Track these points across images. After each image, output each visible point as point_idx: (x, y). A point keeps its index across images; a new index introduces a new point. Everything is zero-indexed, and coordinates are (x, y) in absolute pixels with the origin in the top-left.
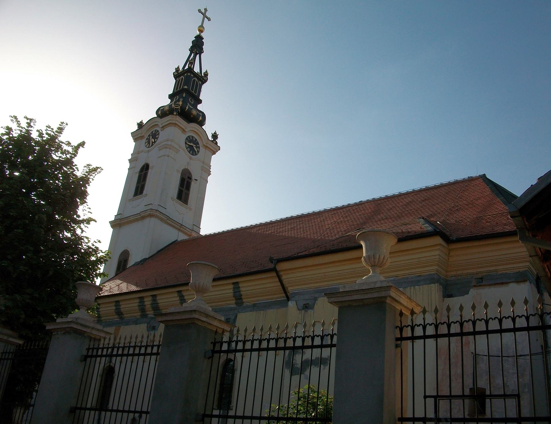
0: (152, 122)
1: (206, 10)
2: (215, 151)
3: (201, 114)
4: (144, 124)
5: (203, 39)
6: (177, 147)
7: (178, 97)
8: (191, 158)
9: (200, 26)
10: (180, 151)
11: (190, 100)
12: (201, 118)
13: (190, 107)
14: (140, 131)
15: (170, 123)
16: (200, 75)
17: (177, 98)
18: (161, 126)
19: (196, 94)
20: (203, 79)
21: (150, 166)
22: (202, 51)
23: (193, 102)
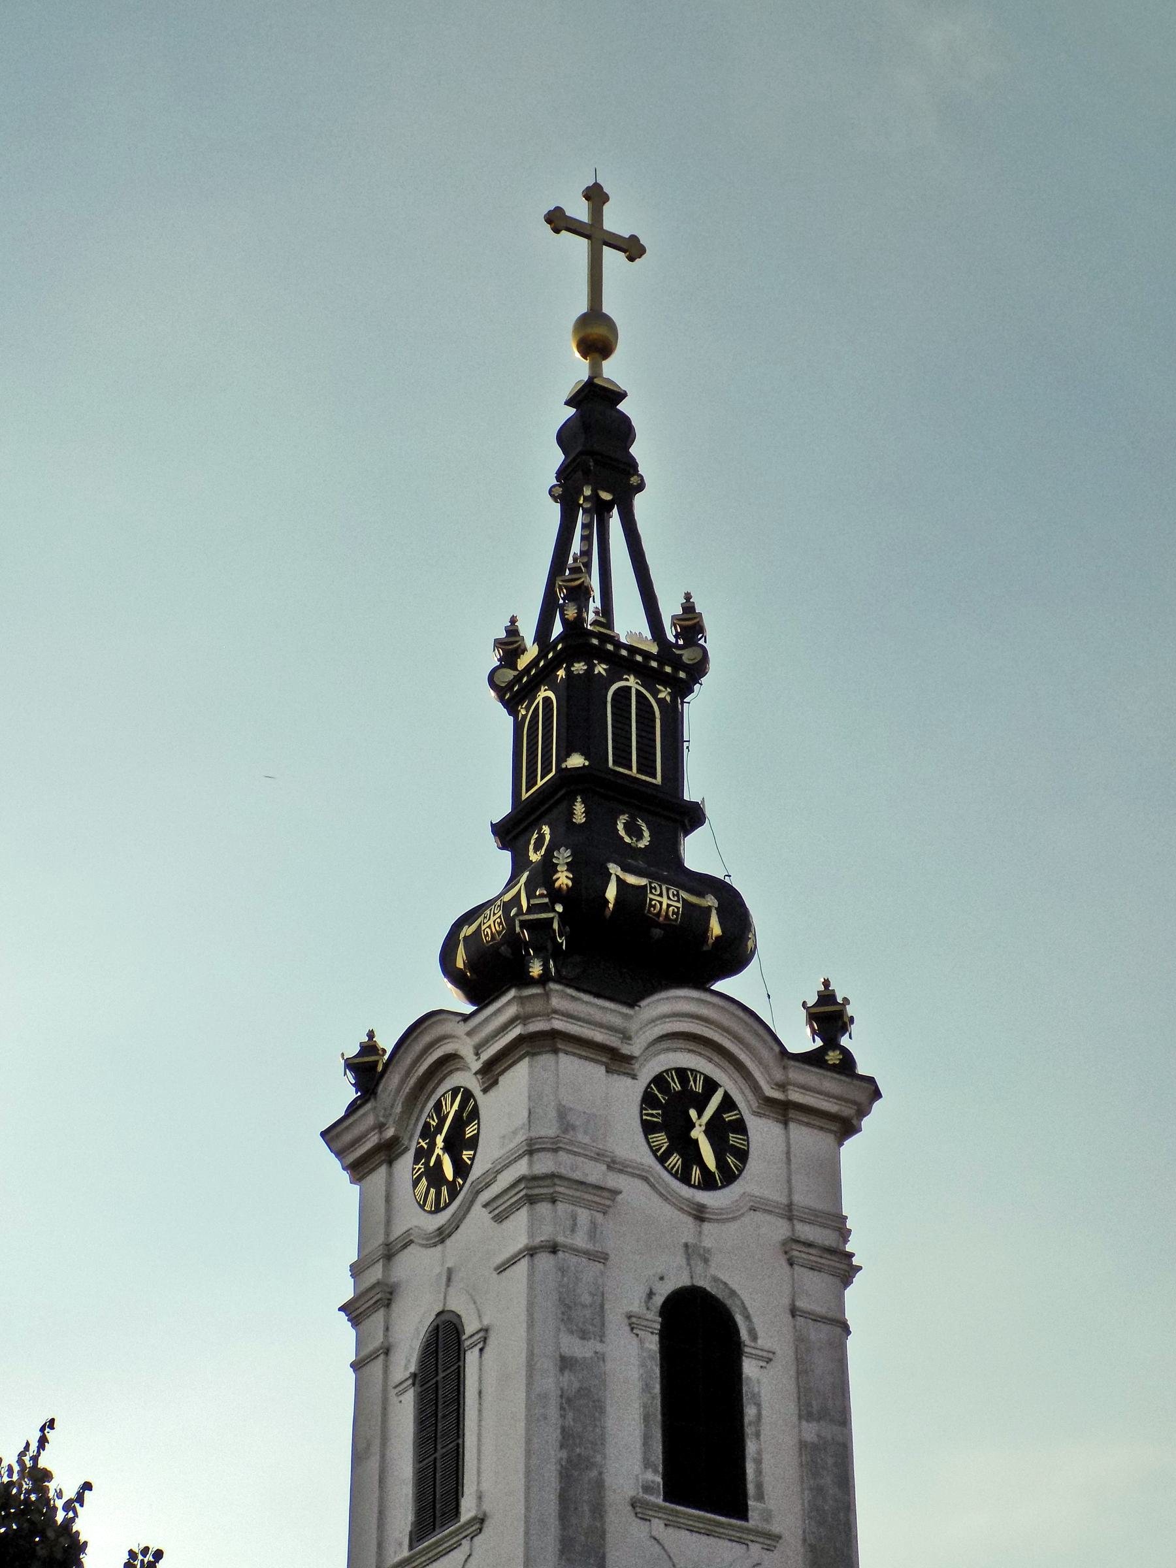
0: (418, 1047)
1: (596, 196)
2: (848, 1111)
3: (711, 901)
4: (386, 1057)
5: (622, 396)
6: (595, 1173)
7: (546, 830)
8: (700, 1214)
9: (584, 322)
10: (618, 1192)
11: (622, 833)
12: (716, 929)
13: (632, 879)
14: (367, 1118)
15: (520, 1040)
16: (654, 650)
17: (541, 837)
18: (476, 1065)
19: (654, 777)
20: (678, 664)
21: (470, 1326)
22: (634, 480)
23: (646, 834)
